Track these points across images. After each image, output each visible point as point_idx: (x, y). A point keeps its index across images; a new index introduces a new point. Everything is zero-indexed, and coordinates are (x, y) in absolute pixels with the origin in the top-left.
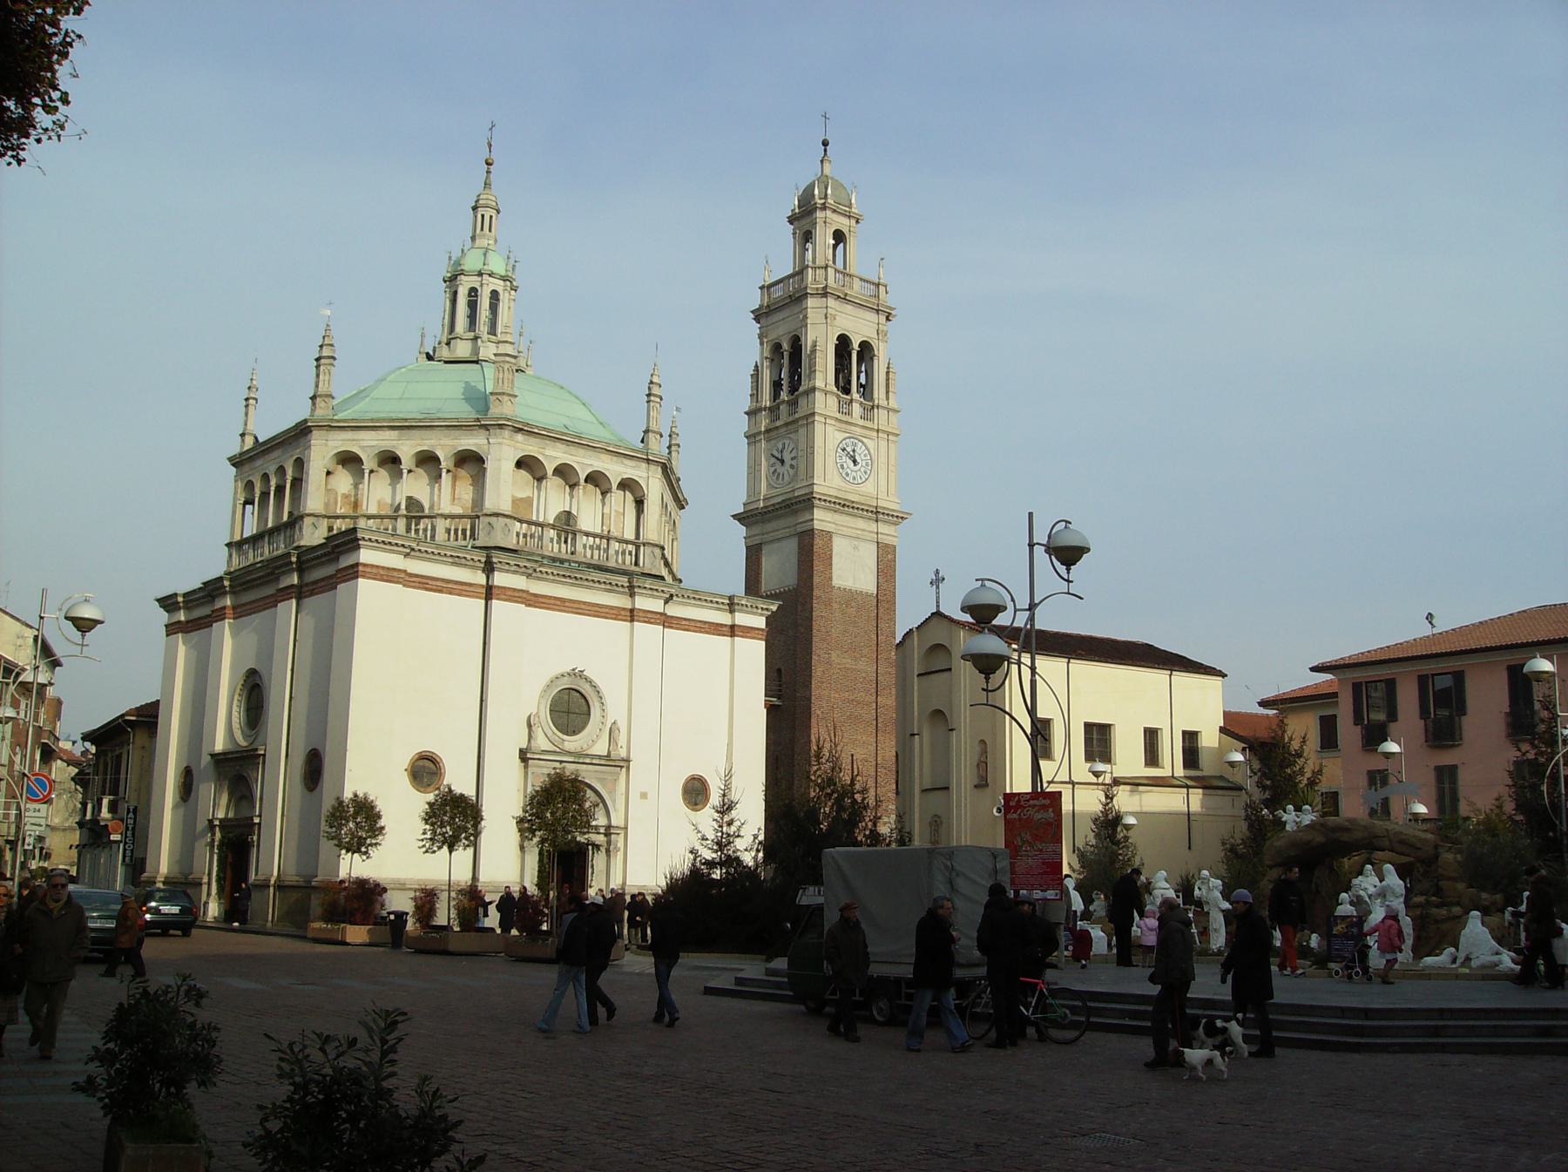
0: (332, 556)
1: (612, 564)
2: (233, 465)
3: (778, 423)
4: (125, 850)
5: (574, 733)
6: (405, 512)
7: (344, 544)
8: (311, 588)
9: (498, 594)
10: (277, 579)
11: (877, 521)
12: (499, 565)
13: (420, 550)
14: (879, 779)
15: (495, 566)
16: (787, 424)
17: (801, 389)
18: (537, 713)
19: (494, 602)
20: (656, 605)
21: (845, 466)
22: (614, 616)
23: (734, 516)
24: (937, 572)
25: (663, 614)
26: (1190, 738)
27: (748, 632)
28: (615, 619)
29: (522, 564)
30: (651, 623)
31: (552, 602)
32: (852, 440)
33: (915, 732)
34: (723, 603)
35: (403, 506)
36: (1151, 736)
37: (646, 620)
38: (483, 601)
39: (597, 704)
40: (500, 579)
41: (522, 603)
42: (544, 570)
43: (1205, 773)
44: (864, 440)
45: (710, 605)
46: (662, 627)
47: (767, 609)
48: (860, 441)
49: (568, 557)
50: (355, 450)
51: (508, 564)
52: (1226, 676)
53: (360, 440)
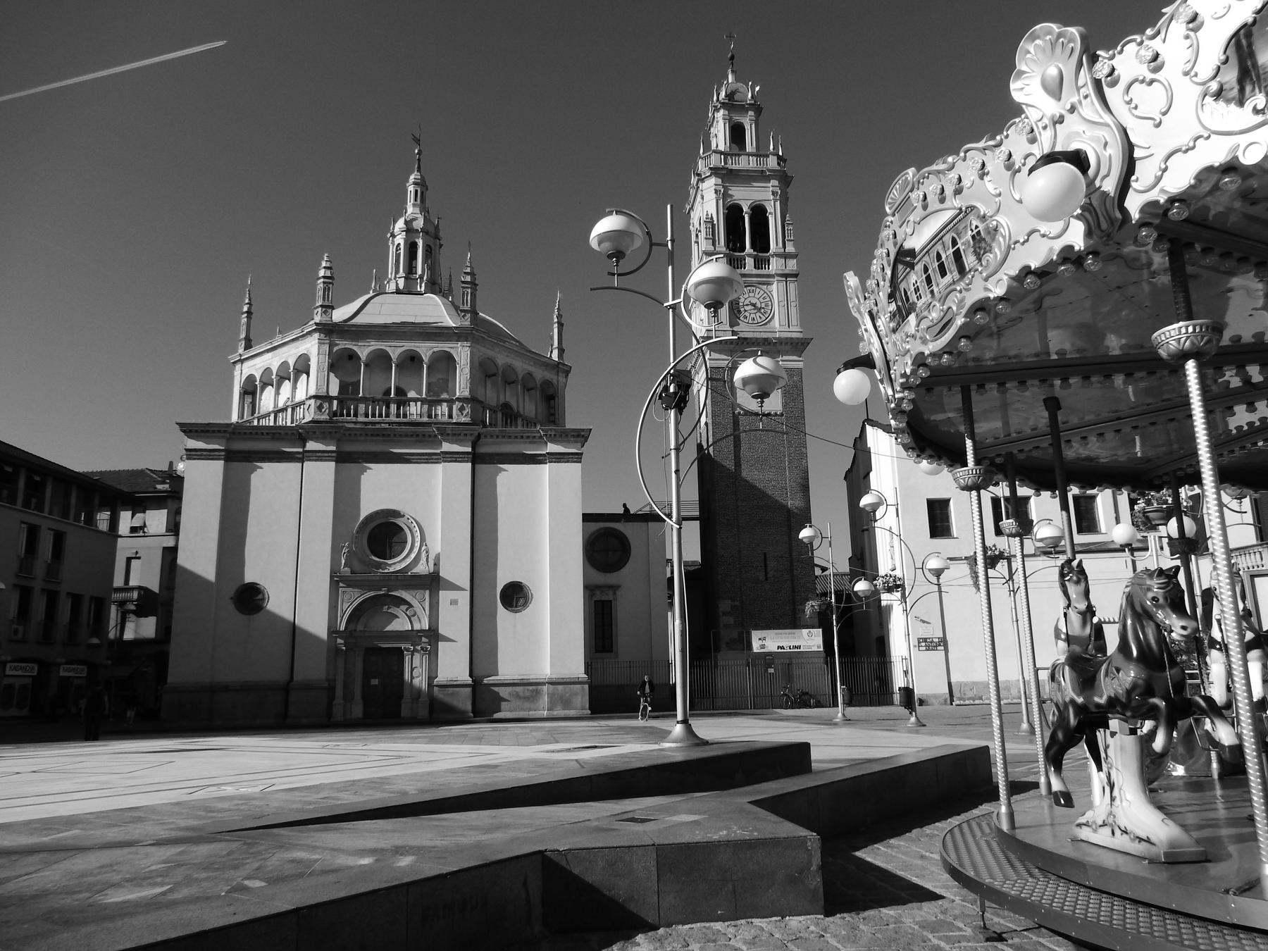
1: (425, 419)
5: (394, 557)
13: (239, 433)
19: (306, 464)
22: (426, 461)
32: (749, 288)
34: (534, 437)
37: (454, 459)
38: (301, 464)
41: (332, 461)
42: (352, 433)
44: (761, 286)
45: (522, 440)
46: (469, 465)
47: (578, 436)
51: (315, 432)
53: (255, 365)
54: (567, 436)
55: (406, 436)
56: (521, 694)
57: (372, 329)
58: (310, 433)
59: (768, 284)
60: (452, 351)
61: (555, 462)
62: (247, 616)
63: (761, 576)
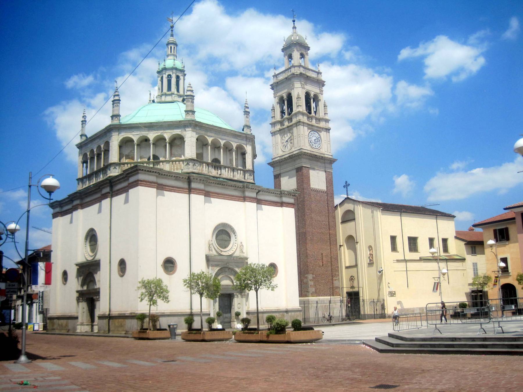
0: (126, 178)
2: (78, 148)
3: (284, 127)
4: (39, 306)
5: (225, 247)
6: (152, 160)
7: (131, 172)
8: (117, 192)
9: (194, 192)
10: (101, 191)
11: (325, 163)
12: (193, 180)
13: (162, 174)
14: (333, 263)
15: (192, 180)
16: (288, 127)
17: (293, 113)
18: (212, 241)
20: (254, 195)
21: (312, 142)
22: (238, 200)
23: (269, 164)
24: (346, 182)
25: (256, 198)
26: (445, 241)
27: (288, 205)
28: (238, 201)
29: (202, 179)
30: (252, 202)
31: (214, 194)
33: (341, 245)
35: (151, 158)
36: (431, 240)
37: (250, 201)
38: (188, 195)
39: (233, 235)
40: (193, 185)
42: (210, 181)
43: (451, 254)
45: (273, 194)
47: (294, 196)
48: (316, 132)
49: (218, 176)
50: (131, 136)
51: (197, 179)
52: (455, 217)
54: (291, 195)
55: (231, 186)
56: (278, 316)
57: (215, 128)
58: (195, 179)
59: (321, 132)
60: (245, 146)
61: (286, 207)
62: (169, 276)
63: (321, 265)
